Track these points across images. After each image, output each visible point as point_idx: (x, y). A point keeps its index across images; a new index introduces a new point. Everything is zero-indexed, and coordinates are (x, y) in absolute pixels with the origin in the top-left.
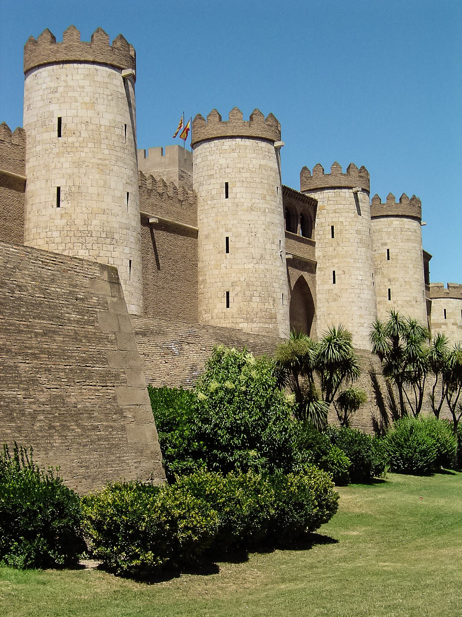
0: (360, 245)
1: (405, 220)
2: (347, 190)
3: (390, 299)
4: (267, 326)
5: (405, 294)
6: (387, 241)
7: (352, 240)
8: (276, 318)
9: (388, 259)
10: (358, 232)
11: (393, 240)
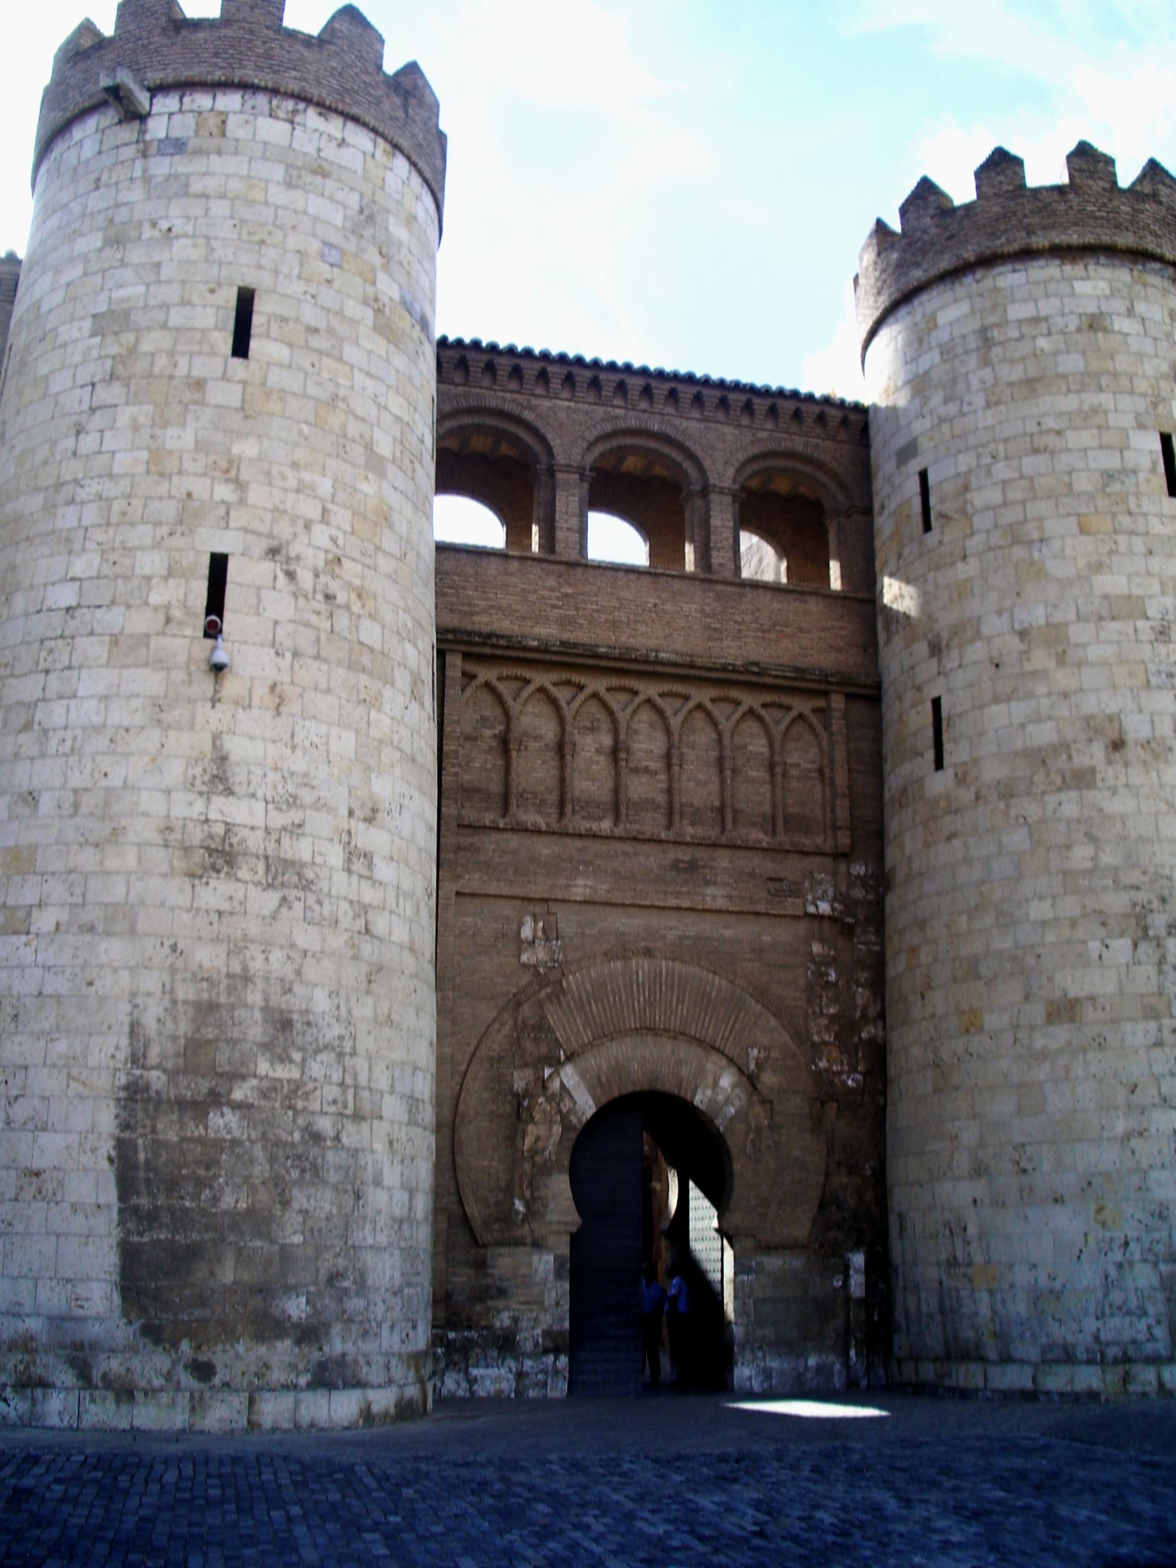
0: (105, 394)
1: (1008, 278)
3: (939, 764)
5: (1019, 709)
9: (927, 527)
11: (943, 411)
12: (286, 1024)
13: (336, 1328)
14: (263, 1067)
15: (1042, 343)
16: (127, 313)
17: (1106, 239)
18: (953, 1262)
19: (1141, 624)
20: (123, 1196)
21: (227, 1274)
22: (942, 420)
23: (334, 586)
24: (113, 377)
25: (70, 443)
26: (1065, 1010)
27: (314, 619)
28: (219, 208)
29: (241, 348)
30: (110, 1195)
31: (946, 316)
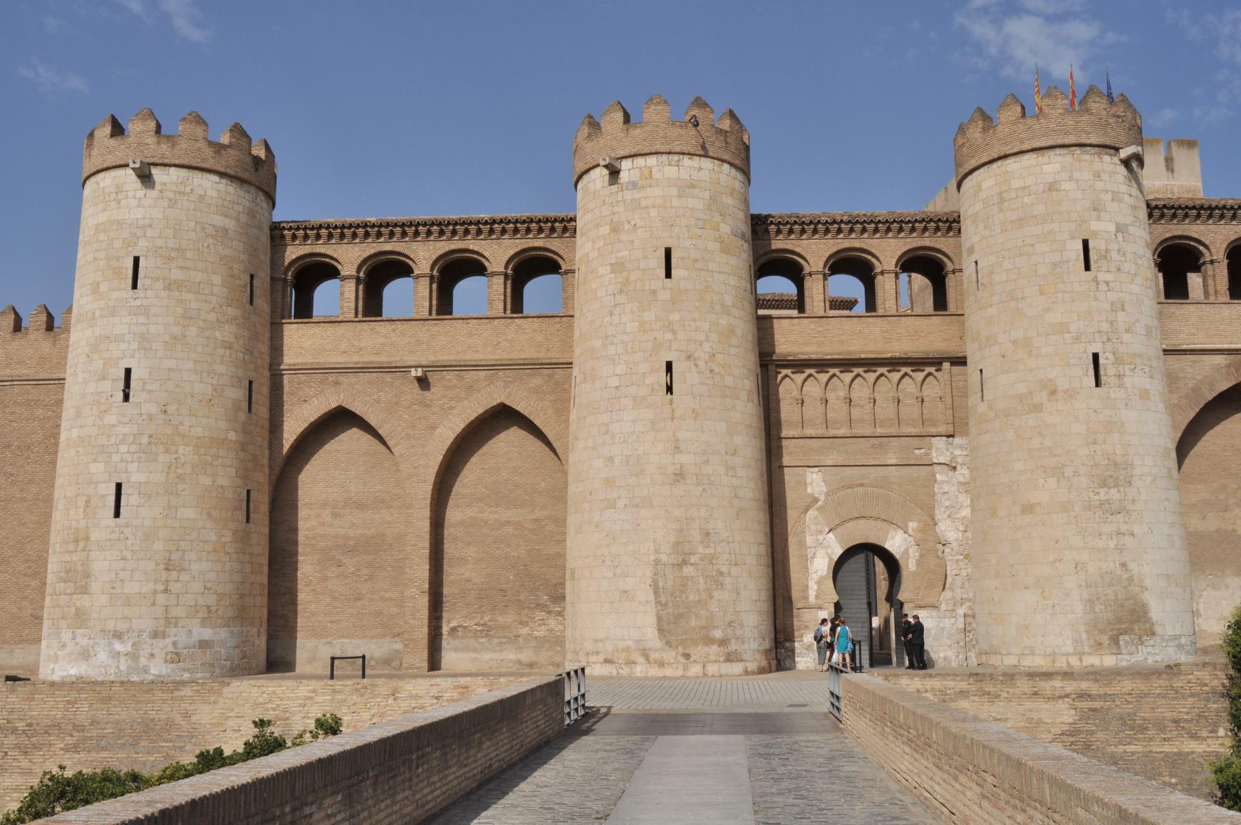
0: (621, 299)
1: (1011, 164)
2: (598, 170)
4: (67, 558)
6: (975, 239)
7: (601, 293)
8: (87, 539)
10: (618, 267)
12: (708, 534)
13: (733, 641)
14: (701, 550)
15: (1026, 200)
16: (623, 263)
17: (1060, 142)
18: (990, 613)
19: (1066, 336)
20: (656, 597)
21: (693, 623)
22: (984, 238)
23: (713, 365)
24: (621, 291)
25: (608, 319)
26: (1028, 509)
27: (707, 381)
28: (654, 212)
29: (668, 275)
30: (652, 597)
31: (985, 185)
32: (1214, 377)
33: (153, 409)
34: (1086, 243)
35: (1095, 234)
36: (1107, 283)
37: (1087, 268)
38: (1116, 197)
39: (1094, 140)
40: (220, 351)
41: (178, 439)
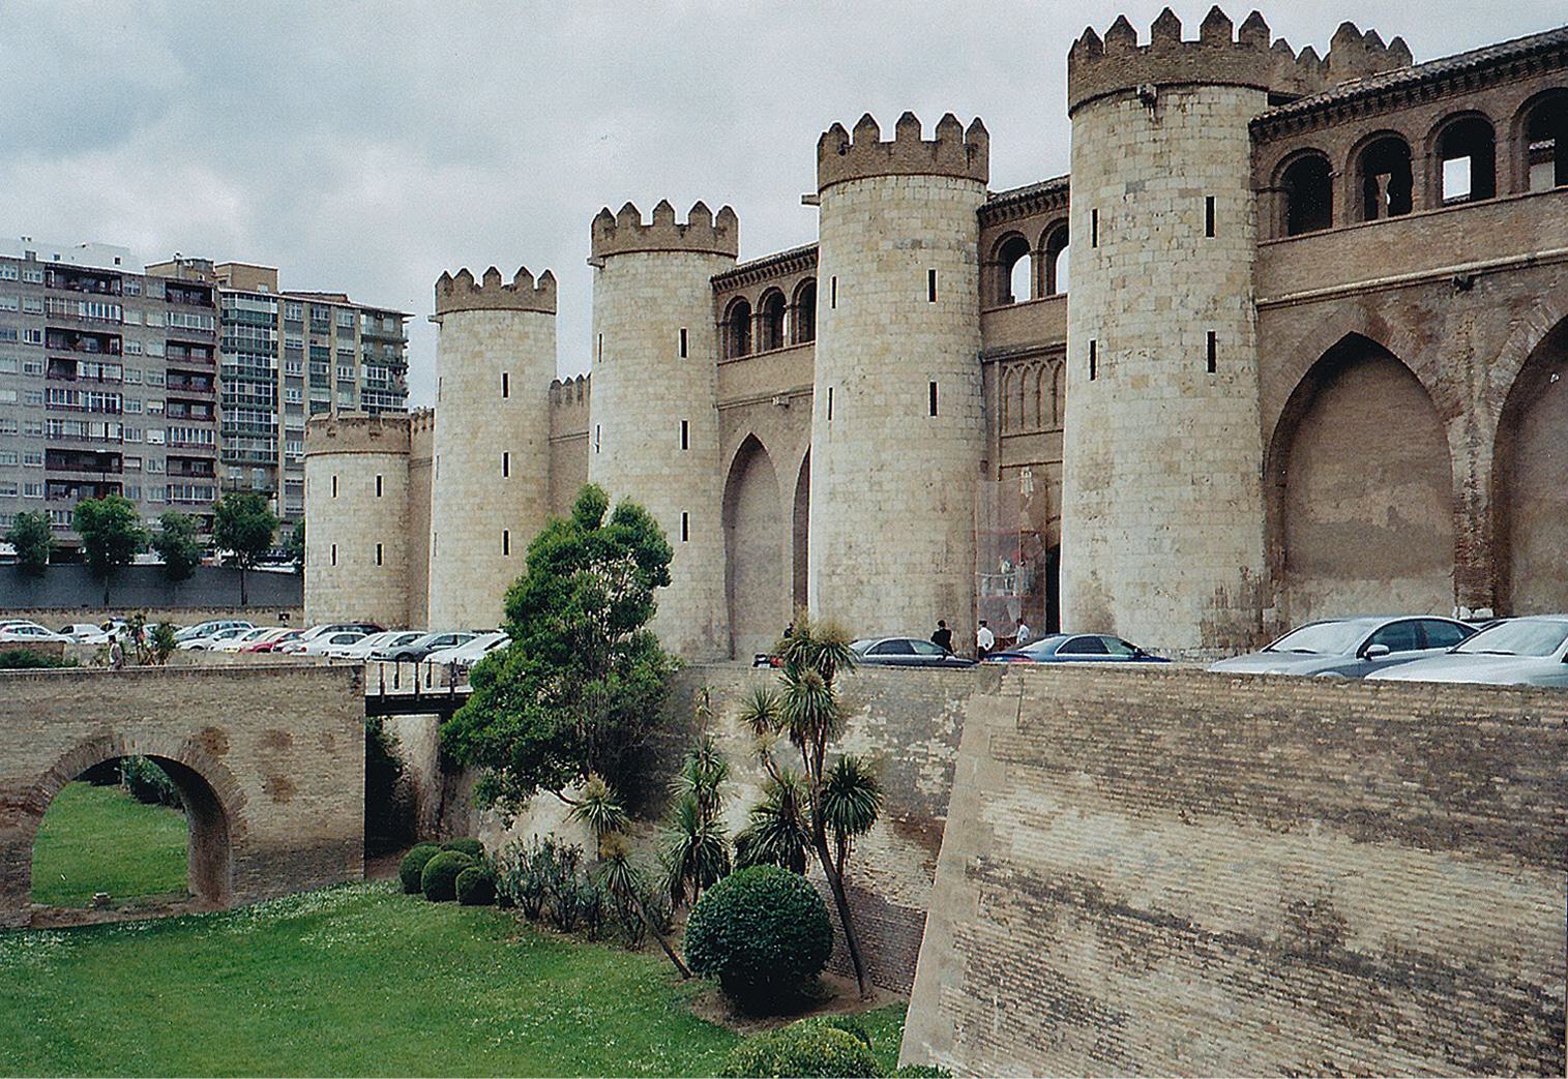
23: (862, 387)
32: (1314, 333)
33: (609, 457)
34: (1095, 212)
35: (1104, 200)
36: (1109, 258)
37: (1095, 245)
38: (1132, 151)
39: (1108, 87)
40: (652, 403)
41: (623, 479)
